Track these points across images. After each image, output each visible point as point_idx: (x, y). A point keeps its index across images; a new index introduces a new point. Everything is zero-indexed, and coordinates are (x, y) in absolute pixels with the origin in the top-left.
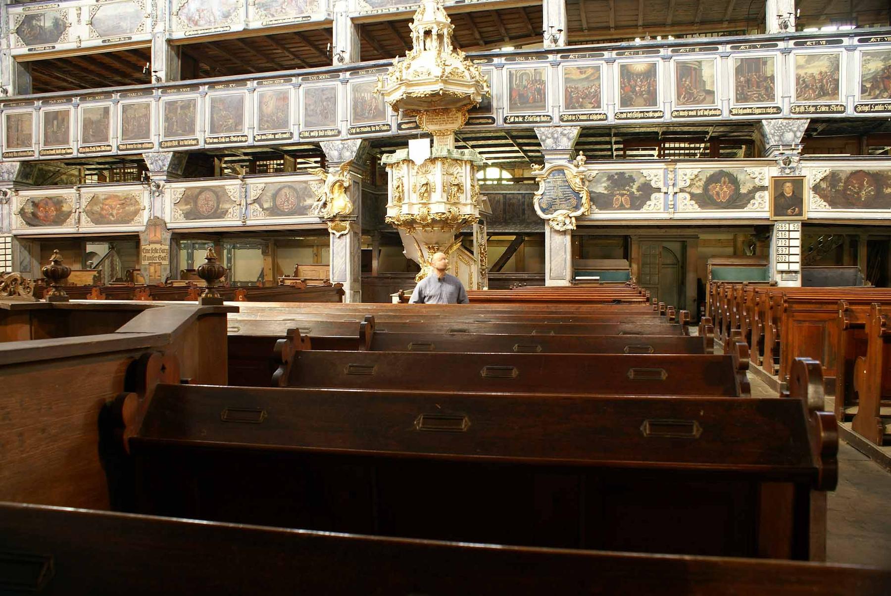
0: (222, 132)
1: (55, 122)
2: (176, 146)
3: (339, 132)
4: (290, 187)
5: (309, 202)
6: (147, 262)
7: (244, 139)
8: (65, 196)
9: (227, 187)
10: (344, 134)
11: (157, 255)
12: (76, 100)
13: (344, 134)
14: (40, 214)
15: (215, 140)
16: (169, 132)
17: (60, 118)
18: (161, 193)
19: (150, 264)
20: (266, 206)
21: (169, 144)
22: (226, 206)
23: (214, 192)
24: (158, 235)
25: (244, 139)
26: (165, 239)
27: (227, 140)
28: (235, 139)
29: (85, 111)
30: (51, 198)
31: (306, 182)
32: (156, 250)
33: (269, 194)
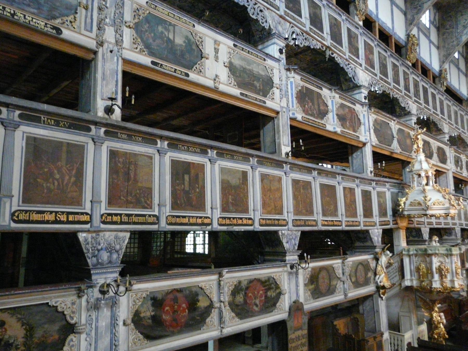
1: (187, 177)
2: (302, 226)
3: (376, 224)
8: (202, 285)
9: (334, 266)
10: (378, 224)
12: (212, 153)
13: (378, 224)
14: (166, 317)
17: (193, 172)
18: (297, 273)
26: (305, 323)
29: (223, 170)
30: (180, 291)
31: (367, 260)
33: (354, 271)
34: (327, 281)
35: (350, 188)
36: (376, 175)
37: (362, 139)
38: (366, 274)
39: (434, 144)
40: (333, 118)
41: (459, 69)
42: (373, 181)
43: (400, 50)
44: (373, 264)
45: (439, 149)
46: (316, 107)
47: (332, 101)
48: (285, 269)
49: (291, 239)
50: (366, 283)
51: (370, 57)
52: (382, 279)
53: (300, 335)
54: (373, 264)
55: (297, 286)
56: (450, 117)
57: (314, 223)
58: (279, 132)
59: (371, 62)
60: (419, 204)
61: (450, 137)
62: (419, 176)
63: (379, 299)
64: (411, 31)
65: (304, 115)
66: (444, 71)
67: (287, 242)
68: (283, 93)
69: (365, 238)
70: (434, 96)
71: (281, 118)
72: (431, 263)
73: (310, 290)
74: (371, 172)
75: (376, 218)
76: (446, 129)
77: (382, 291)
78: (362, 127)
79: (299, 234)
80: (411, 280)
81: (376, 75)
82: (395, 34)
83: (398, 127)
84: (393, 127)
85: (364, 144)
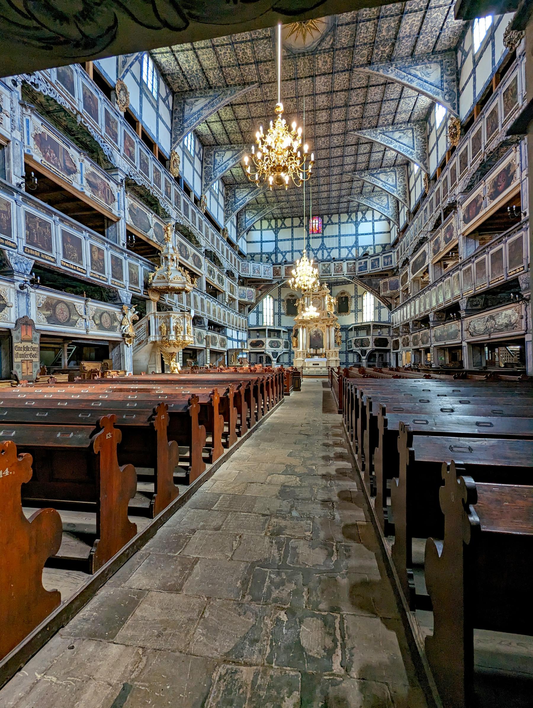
0: (71, 260)
2: (36, 256)
3: (125, 287)
4: (106, 312)
5: (116, 324)
6: (19, 360)
7: (84, 272)
9: (76, 304)
11: (28, 352)
15: (67, 265)
16: (30, 240)
18: (28, 295)
19: (22, 362)
20: (97, 322)
21: (32, 252)
22: (75, 318)
23: (66, 304)
24: (29, 333)
25: (84, 272)
27: (75, 268)
28: (79, 270)
32: (27, 349)
34: (66, 313)
35: (99, 249)
36: (128, 247)
37: (115, 212)
38: (112, 323)
39: (191, 250)
40: (82, 179)
41: (218, 203)
42: (125, 252)
43: (163, 160)
44: (119, 317)
45: (195, 255)
46: (61, 160)
47: (81, 164)
48: (12, 285)
49: (21, 263)
50: (112, 329)
51: (131, 149)
52: (130, 330)
53: (29, 346)
54: (119, 317)
55: (28, 305)
56: (207, 235)
57: (52, 260)
58: (9, 160)
59: (130, 154)
60: (164, 278)
61: (206, 250)
62: (166, 258)
63: (125, 346)
64: (175, 148)
65: (44, 159)
66: (203, 197)
67: (16, 263)
68: (17, 125)
69: (115, 297)
70: (194, 214)
71: (11, 148)
72: (170, 323)
73: (44, 314)
74: (124, 245)
75: (126, 281)
76: (203, 243)
77: (127, 339)
78: (116, 203)
79: (33, 262)
80: (155, 337)
81: (136, 168)
82: (143, 122)
83: (155, 220)
84: (150, 219)
85: (118, 220)
